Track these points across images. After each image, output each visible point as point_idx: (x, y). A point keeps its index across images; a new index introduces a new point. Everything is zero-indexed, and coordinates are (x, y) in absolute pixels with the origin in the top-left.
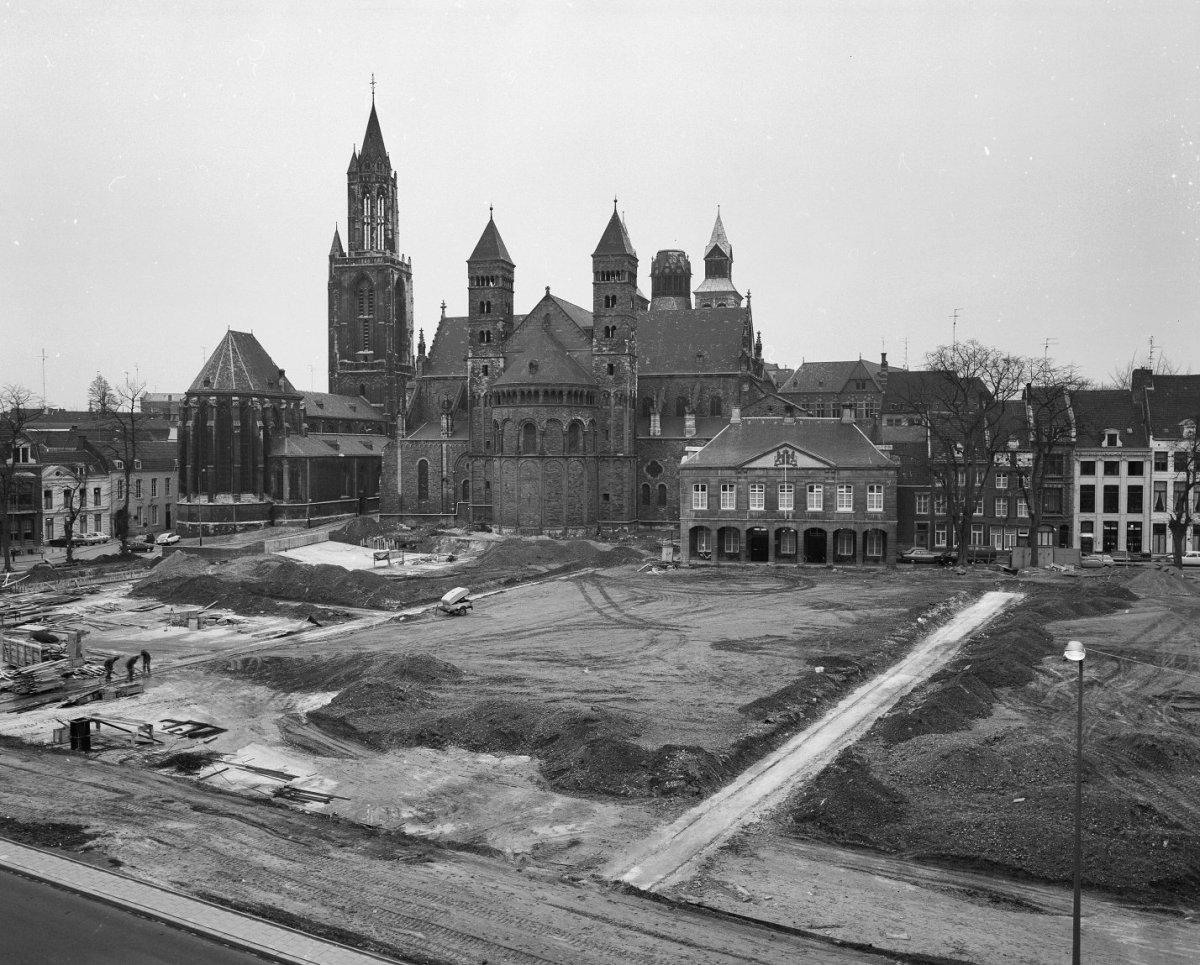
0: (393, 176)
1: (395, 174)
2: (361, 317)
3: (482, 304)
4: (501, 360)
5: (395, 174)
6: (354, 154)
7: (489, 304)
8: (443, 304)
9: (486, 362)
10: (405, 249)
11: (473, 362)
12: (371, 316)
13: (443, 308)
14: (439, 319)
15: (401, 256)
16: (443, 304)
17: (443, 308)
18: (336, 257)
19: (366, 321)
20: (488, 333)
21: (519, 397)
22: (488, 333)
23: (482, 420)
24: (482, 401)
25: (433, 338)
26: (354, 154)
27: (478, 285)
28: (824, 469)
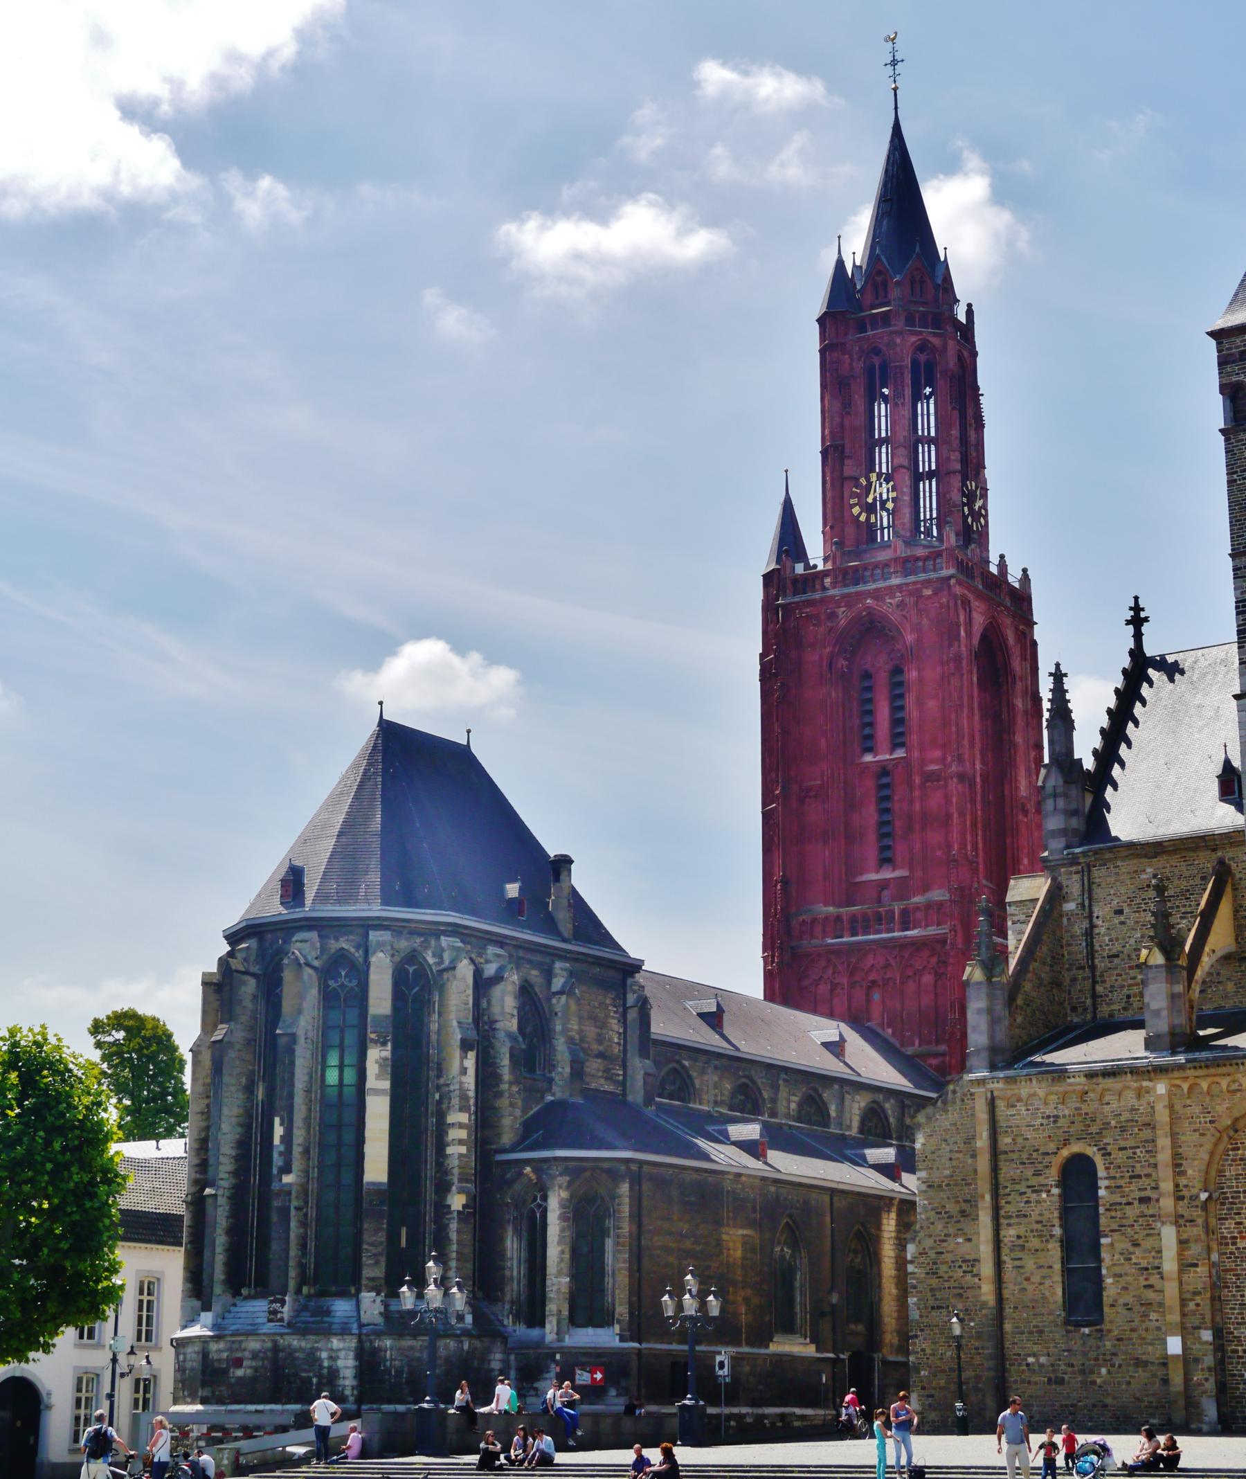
0: (962, 317)
1: (970, 312)
2: (868, 758)
5: (970, 312)
6: (840, 264)
8: (1137, 608)
10: (1010, 542)
12: (900, 753)
13: (1137, 620)
14: (1126, 662)
15: (994, 559)
16: (1137, 608)
17: (1137, 620)
18: (786, 589)
19: (884, 770)
26: (840, 264)
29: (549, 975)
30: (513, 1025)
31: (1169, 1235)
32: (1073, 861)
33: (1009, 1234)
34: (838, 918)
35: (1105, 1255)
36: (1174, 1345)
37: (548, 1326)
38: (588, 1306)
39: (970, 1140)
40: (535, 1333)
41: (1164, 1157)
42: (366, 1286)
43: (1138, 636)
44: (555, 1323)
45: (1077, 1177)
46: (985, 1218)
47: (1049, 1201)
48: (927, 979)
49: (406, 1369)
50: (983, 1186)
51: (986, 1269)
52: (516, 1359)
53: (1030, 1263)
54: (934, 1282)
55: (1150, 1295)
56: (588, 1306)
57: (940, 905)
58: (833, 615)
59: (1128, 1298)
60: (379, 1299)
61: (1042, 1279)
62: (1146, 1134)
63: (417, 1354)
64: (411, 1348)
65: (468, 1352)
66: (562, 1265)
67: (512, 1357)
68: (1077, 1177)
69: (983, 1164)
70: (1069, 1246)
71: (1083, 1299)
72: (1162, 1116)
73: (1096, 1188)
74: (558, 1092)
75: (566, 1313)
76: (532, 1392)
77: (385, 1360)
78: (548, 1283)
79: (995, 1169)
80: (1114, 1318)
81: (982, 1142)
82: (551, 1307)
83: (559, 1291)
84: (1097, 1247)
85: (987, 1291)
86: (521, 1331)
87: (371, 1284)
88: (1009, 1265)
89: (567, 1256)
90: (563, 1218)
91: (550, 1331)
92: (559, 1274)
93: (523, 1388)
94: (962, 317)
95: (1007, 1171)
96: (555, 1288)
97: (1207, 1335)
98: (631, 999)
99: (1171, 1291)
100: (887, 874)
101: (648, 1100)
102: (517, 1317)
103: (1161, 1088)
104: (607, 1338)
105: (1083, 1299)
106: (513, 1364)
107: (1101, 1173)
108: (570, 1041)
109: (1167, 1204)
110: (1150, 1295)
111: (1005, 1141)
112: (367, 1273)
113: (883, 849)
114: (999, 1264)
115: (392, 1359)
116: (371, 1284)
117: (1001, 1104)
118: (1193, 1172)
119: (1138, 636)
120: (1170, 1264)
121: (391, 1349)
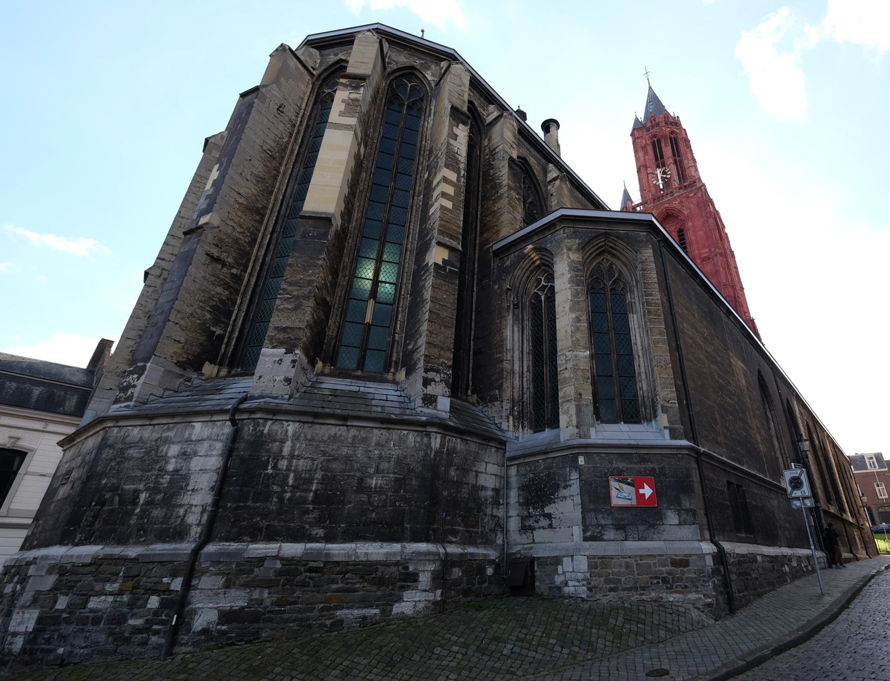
37: (563, 419)
38: (617, 396)
40: (546, 435)
42: (272, 339)
44: (573, 411)
49: (319, 475)
52: (518, 473)
56: (617, 396)
60: (289, 358)
63: (345, 451)
64: (334, 439)
65: (438, 452)
66: (578, 335)
67: (513, 471)
75: (588, 397)
76: (544, 522)
77: (279, 456)
78: (561, 360)
82: (566, 391)
83: (575, 368)
86: (523, 438)
87: (281, 336)
89: (584, 325)
90: (573, 281)
91: (567, 430)
92: (575, 345)
93: (530, 516)
96: (570, 365)
102: (520, 419)
106: (514, 481)
112: (276, 320)
115: (292, 456)
116: (281, 336)
121: (296, 437)
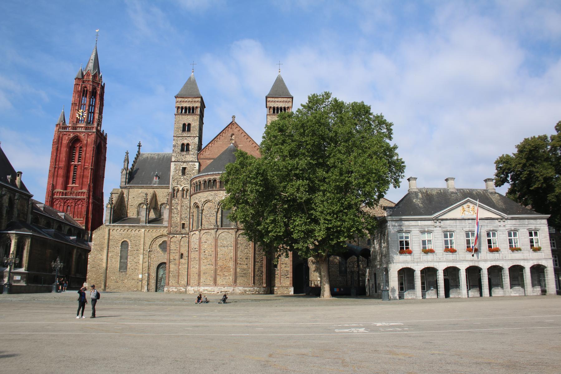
2: (73, 163)
3: (184, 125)
4: (197, 164)
7: (189, 125)
8: (140, 144)
9: (185, 165)
11: (175, 165)
12: (80, 163)
13: (139, 146)
15: (102, 130)
16: (140, 144)
17: (139, 146)
19: (75, 166)
20: (188, 145)
21: (218, 184)
22: (188, 145)
23: (179, 208)
24: (179, 194)
25: (134, 159)
27: (182, 112)
28: (497, 219)
29: (15, 195)
30: (7, 205)
31: (141, 256)
32: (125, 188)
33: (110, 255)
34: (63, 193)
35: (128, 259)
36: (140, 276)
39: (104, 237)
41: (142, 243)
43: (139, 149)
45: (124, 244)
46: (105, 251)
47: (119, 249)
48: (80, 206)
50: (106, 245)
51: (105, 261)
53: (113, 260)
54: (93, 263)
55: (137, 267)
57: (84, 193)
58: (70, 135)
59: (132, 268)
61: (115, 263)
62: (139, 238)
68: (124, 244)
69: (106, 241)
70: (121, 257)
71: (123, 267)
72: (143, 235)
73: (128, 247)
74: (14, 220)
79: (108, 242)
80: (129, 271)
81: (107, 237)
84: (127, 258)
85: (104, 265)
88: (109, 260)
94: (103, 84)
95: (111, 243)
97: (147, 275)
98: (30, 202)
99: (141, 267)
100: (74, 185)
101: (31, 223)
103: (143, 230)
104: (23, 270)
105: (123, 267)
107: (130, 244)
108: (18, 210)
109: (142, 251)
110: (137, 267)
111: (111, 237)
113: (73, 181)
114: (107, 260)
117: (111, 231)
118: (147, 246)
119: (139, 149)
120: (141, 262)
